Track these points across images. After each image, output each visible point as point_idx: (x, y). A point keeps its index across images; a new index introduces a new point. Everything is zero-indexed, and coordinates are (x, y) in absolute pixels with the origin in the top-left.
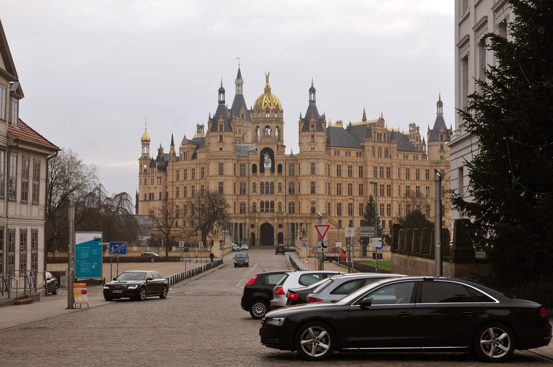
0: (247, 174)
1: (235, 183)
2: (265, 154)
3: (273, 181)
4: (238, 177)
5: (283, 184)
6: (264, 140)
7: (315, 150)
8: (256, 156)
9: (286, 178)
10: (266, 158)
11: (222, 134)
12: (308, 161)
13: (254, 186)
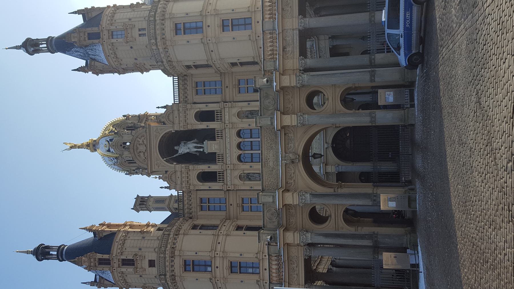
0: (221, 195)
1: (239, 228)
2: (177, 151)
3: (234, 132)
4: (228, 218)
5: (242, 107)
6: (142, 154)
7: (144, 25)
8: (179, 174)
9: (228, 100)
10: (183, 149)
11: (116, 260)
12: (168, 43)
13: (248, 177)
